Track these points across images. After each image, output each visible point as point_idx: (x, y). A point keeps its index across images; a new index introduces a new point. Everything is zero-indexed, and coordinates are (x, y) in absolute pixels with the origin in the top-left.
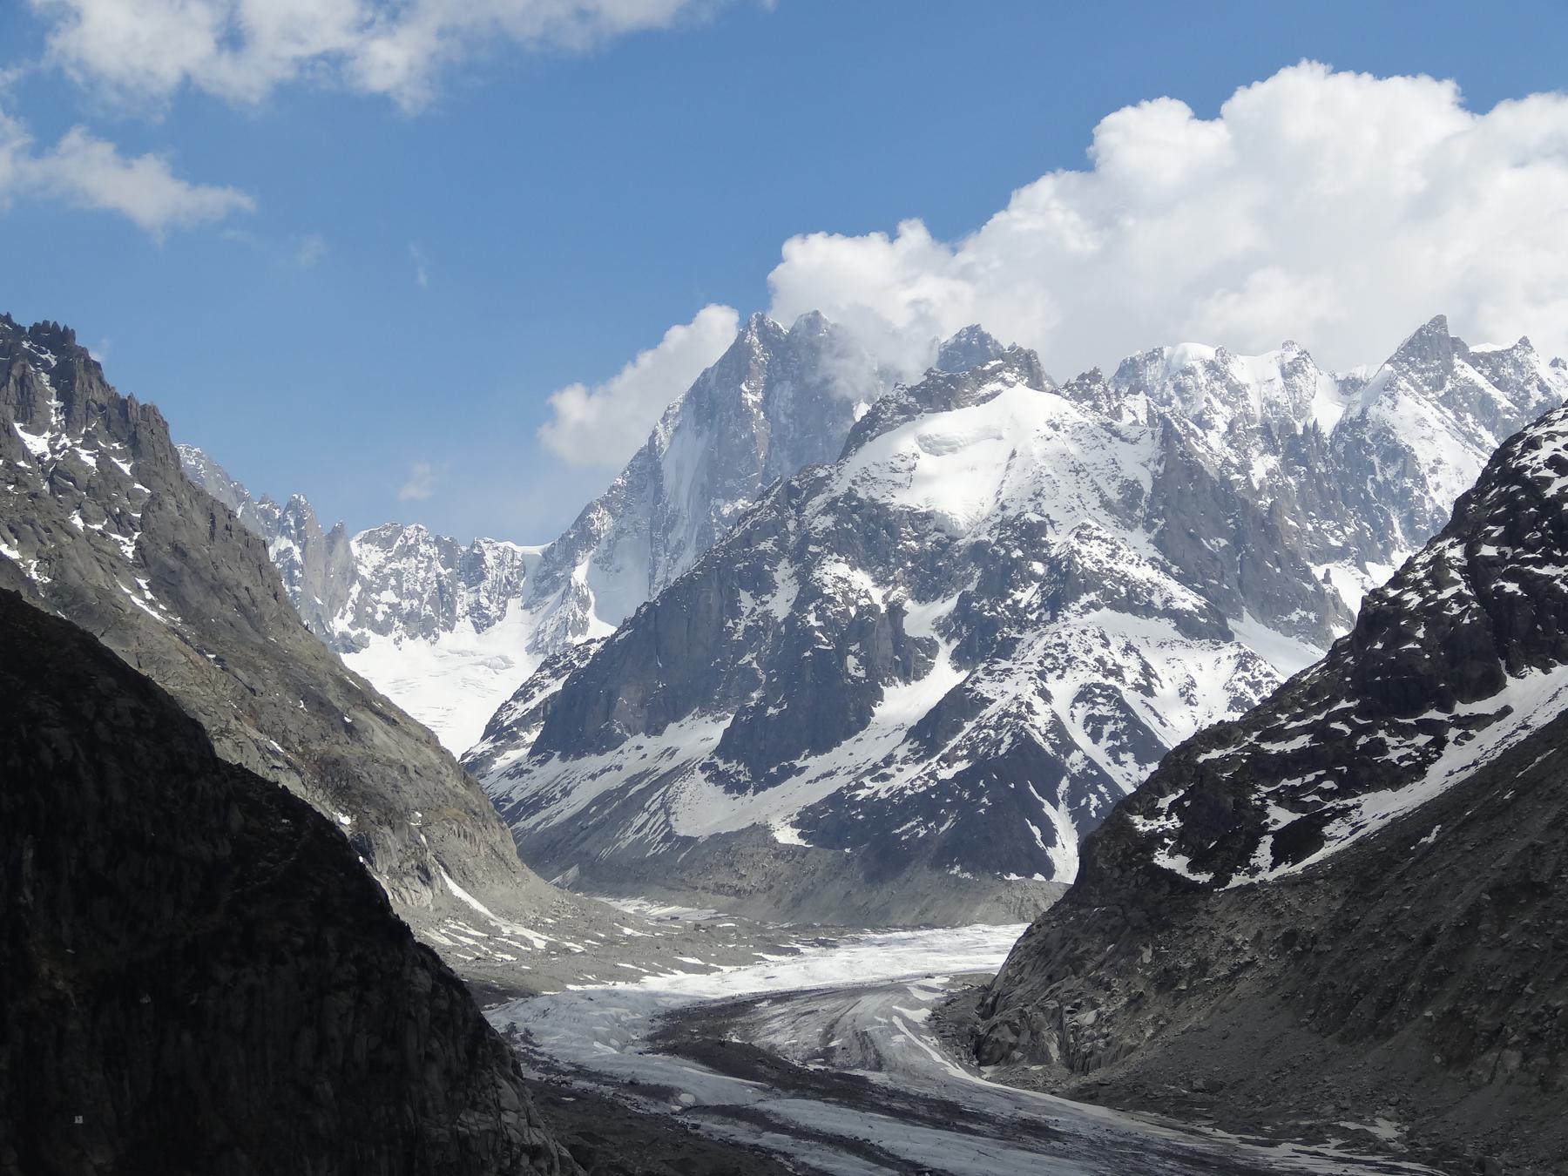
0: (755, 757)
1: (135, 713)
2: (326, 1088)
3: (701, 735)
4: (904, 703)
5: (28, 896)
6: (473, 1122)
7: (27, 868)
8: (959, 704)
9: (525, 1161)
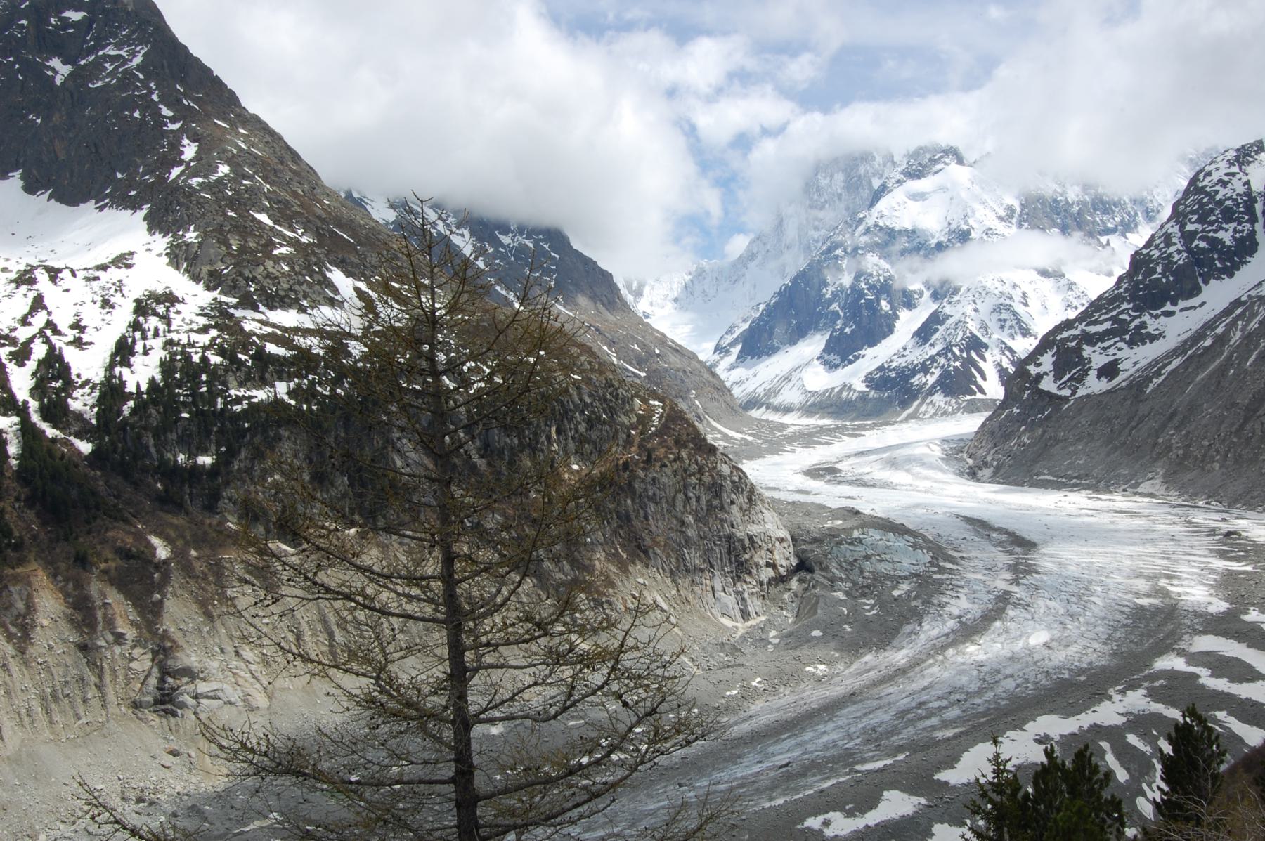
0: (841, 351)
1: (589, 363)
2: (690, 519)
3: (814, 345)
4: (908, 322)
5: (555, 447)
6: (753, 529)
7: (554, 434)
8: (935, 320)
9: (777, 544)
